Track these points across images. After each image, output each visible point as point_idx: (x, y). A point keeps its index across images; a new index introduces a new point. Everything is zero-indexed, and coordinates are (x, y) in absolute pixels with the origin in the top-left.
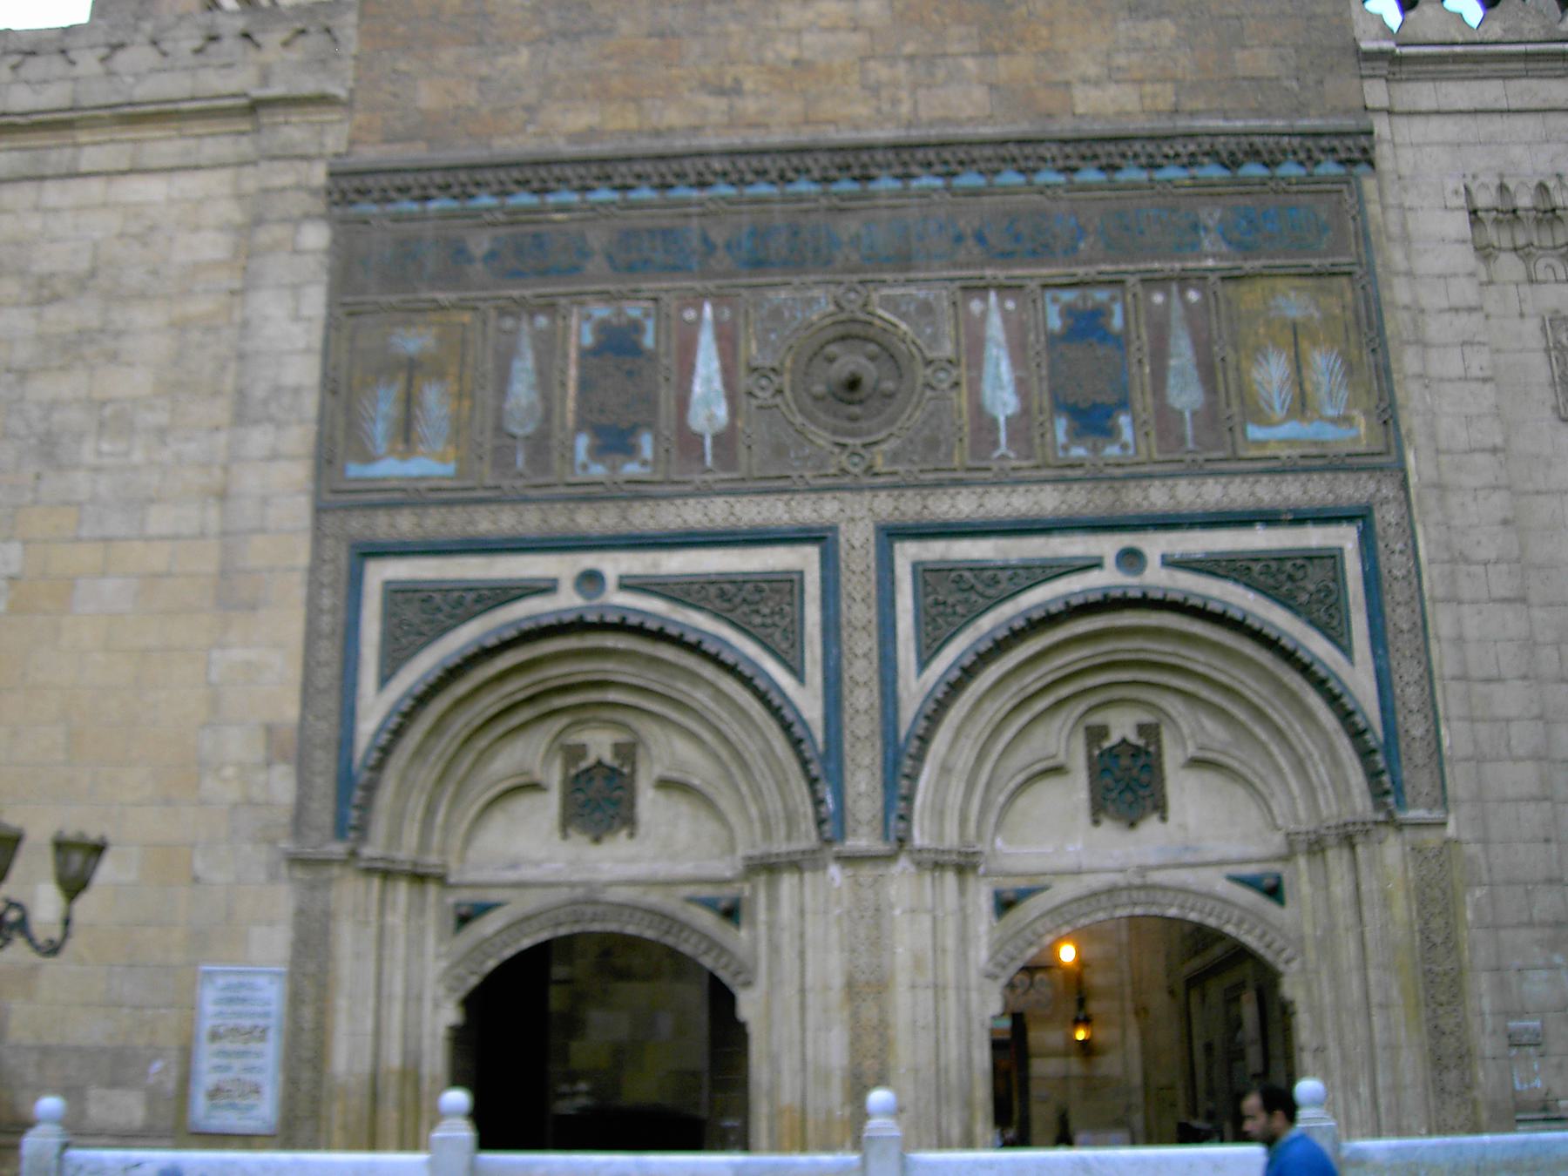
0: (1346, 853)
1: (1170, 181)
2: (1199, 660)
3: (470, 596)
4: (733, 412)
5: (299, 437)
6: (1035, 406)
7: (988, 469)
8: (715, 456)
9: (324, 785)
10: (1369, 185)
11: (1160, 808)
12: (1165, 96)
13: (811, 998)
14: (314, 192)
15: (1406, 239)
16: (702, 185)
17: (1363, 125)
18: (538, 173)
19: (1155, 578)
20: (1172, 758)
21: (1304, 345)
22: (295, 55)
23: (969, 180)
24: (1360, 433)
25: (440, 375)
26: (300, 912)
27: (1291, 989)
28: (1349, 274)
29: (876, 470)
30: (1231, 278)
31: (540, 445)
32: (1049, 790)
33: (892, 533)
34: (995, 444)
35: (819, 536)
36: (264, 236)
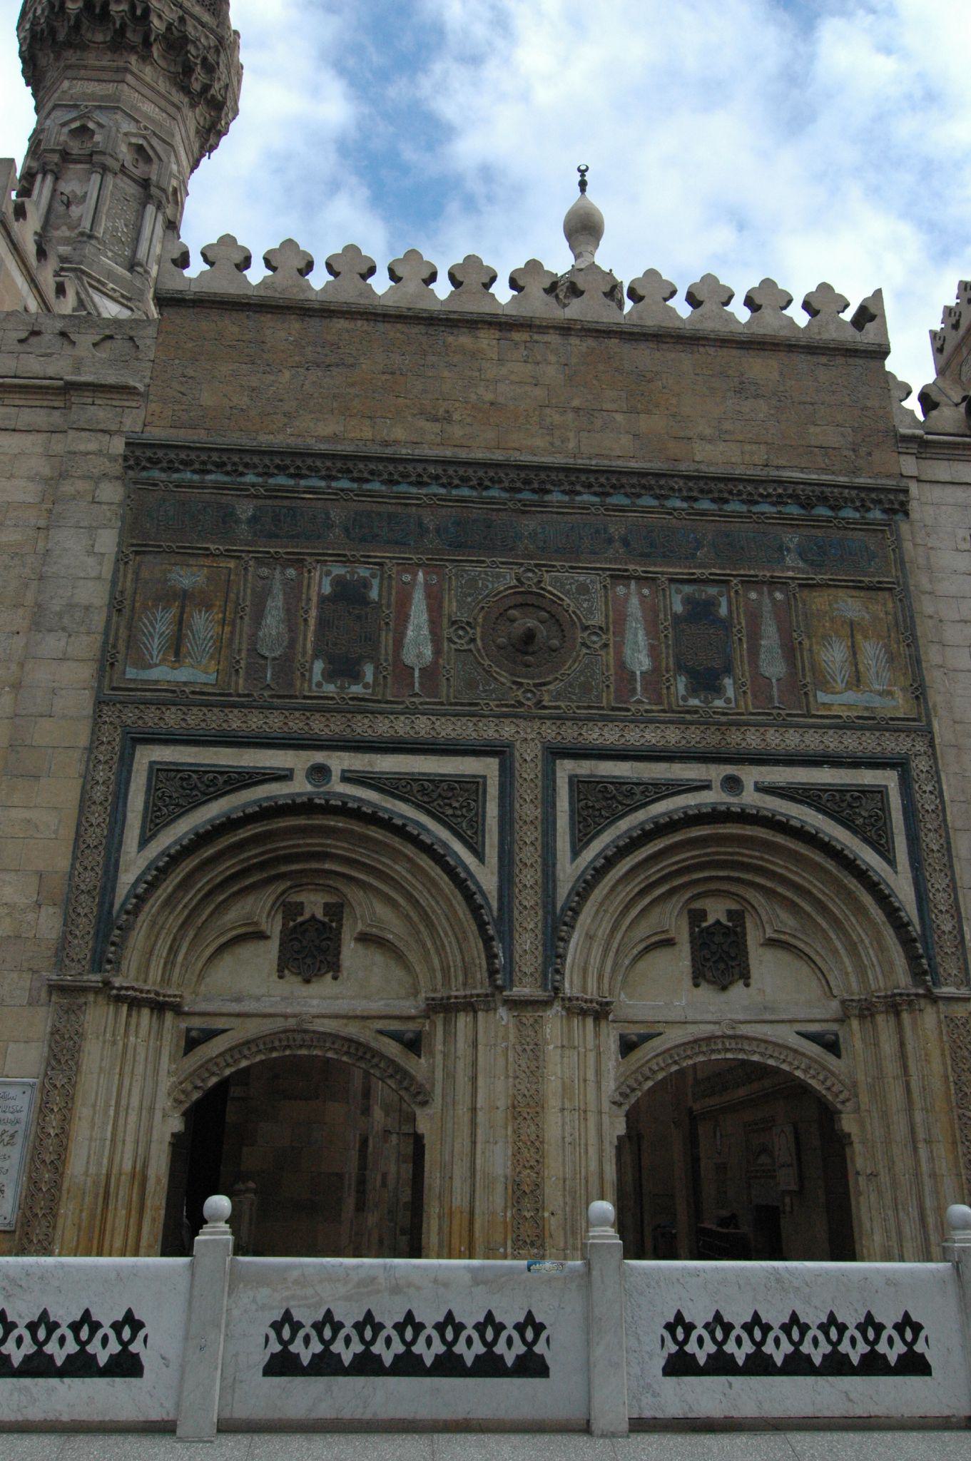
0: (892, 1018)
1: (763, 514)
2: (778, 865)
3: (221, 779)
4: (437, 652)
5: (87, 645)
6: (664, 665)
7: (628, 710)
8: (421, 684)
9: (85, 925)
10: (904, 527)
11: (745, 977)
12: (760, 455)
13: (481, 1117)
14: (113, 459)
15: (929, 568)
16: (420, 484)
18: (295, 461)
19: (750, 798)
20: (753, 938)
21: (859, 637)
22: (102, 354)
23: (618, 499)
24: (899, 705)
25: (209, 607)
26: (55, 1031)
27: (848, 1124)
28: (890, 589)
29: (545, 703)
30: (807, 586)
31: (286, 664)
32: (661, 959)
33: (556, 752)
34: (634, 691)
35: (499, 751)
36: (68, 488)
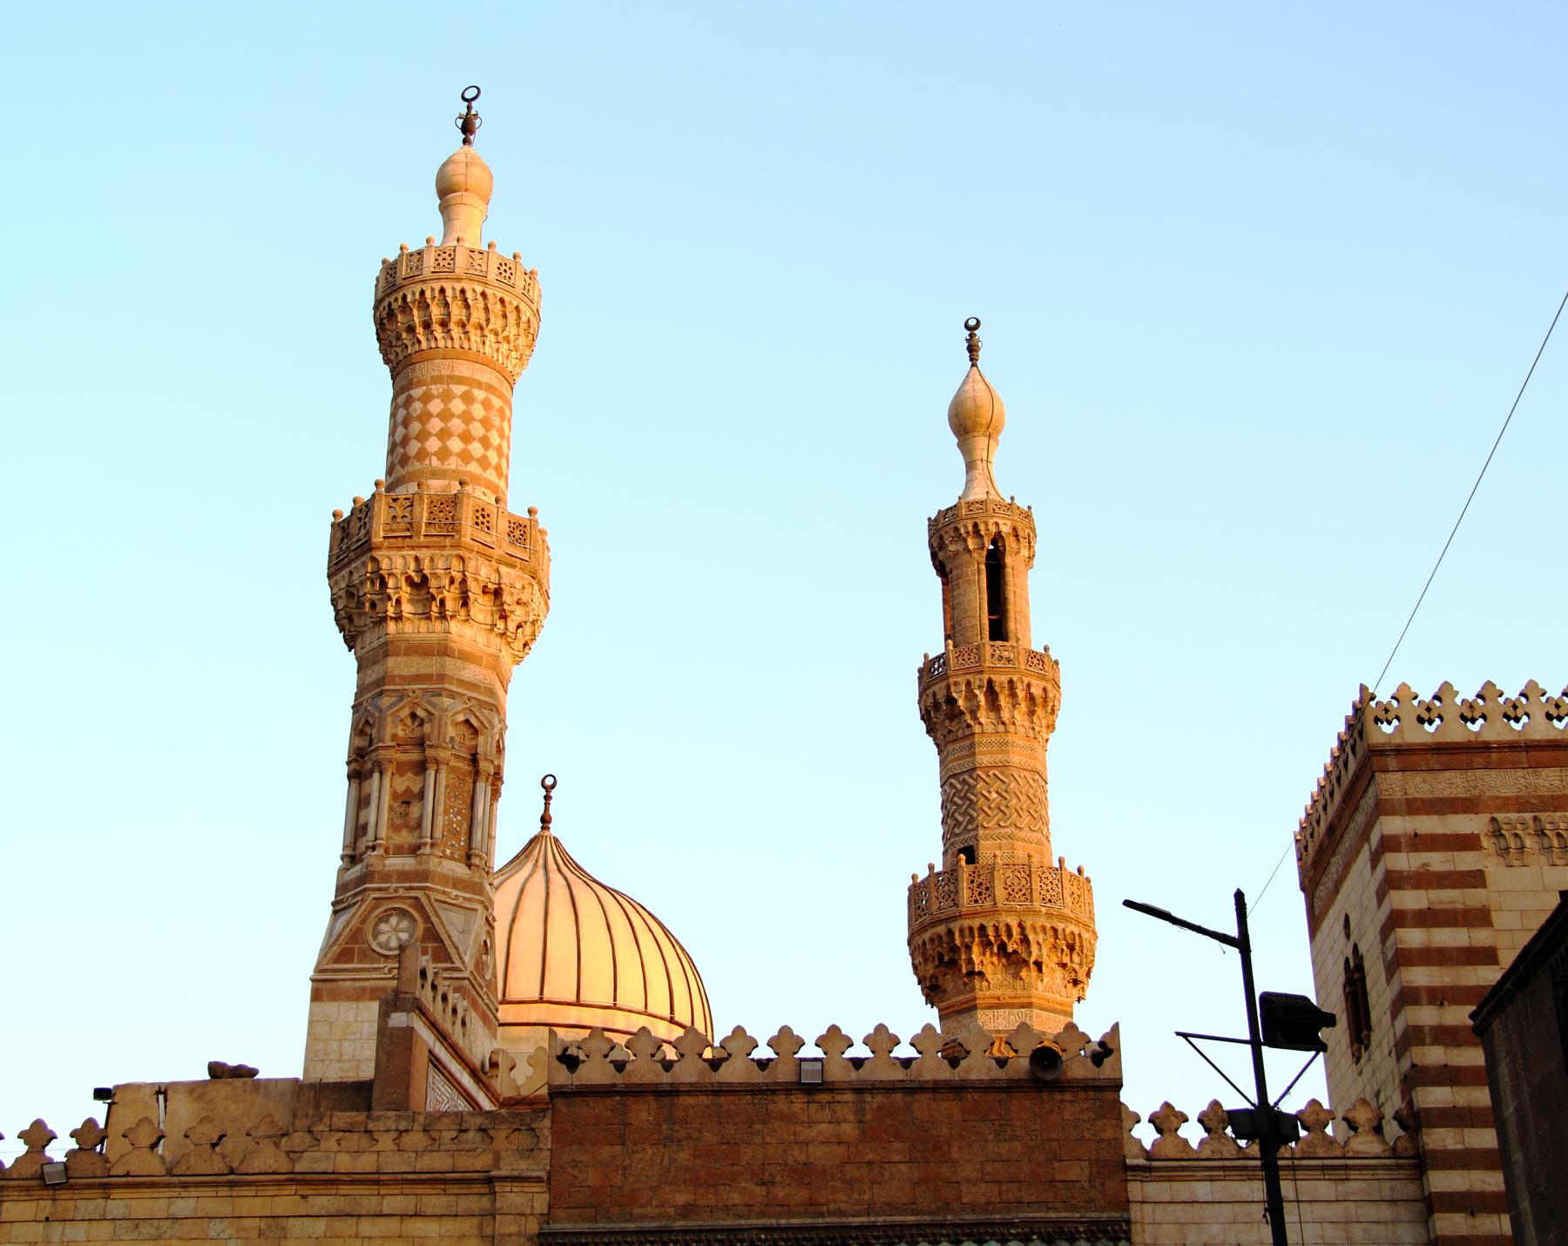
17: (1125, 1215)
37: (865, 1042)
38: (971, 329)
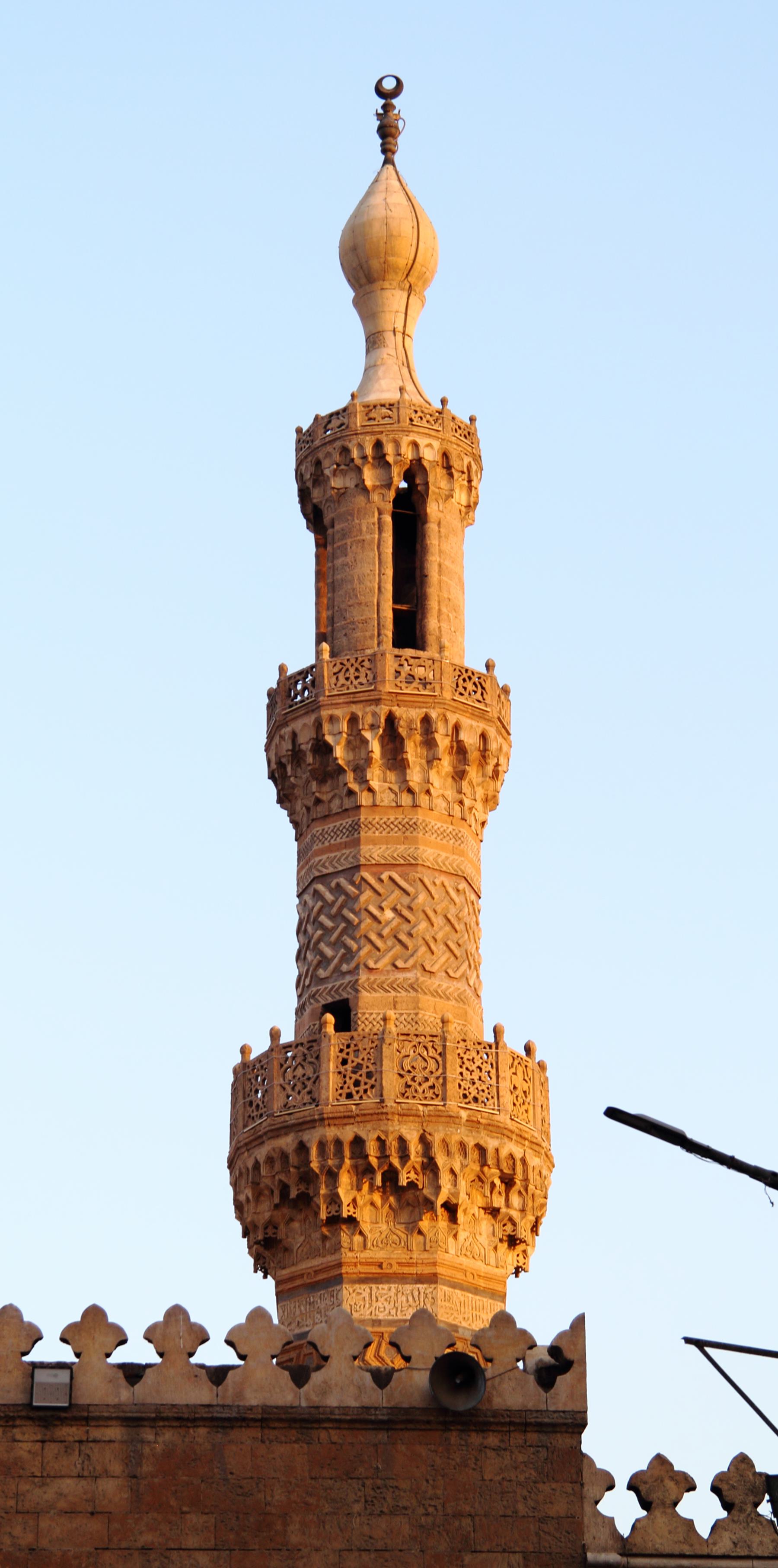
37: (149, 1336)
38: (387, 95)
